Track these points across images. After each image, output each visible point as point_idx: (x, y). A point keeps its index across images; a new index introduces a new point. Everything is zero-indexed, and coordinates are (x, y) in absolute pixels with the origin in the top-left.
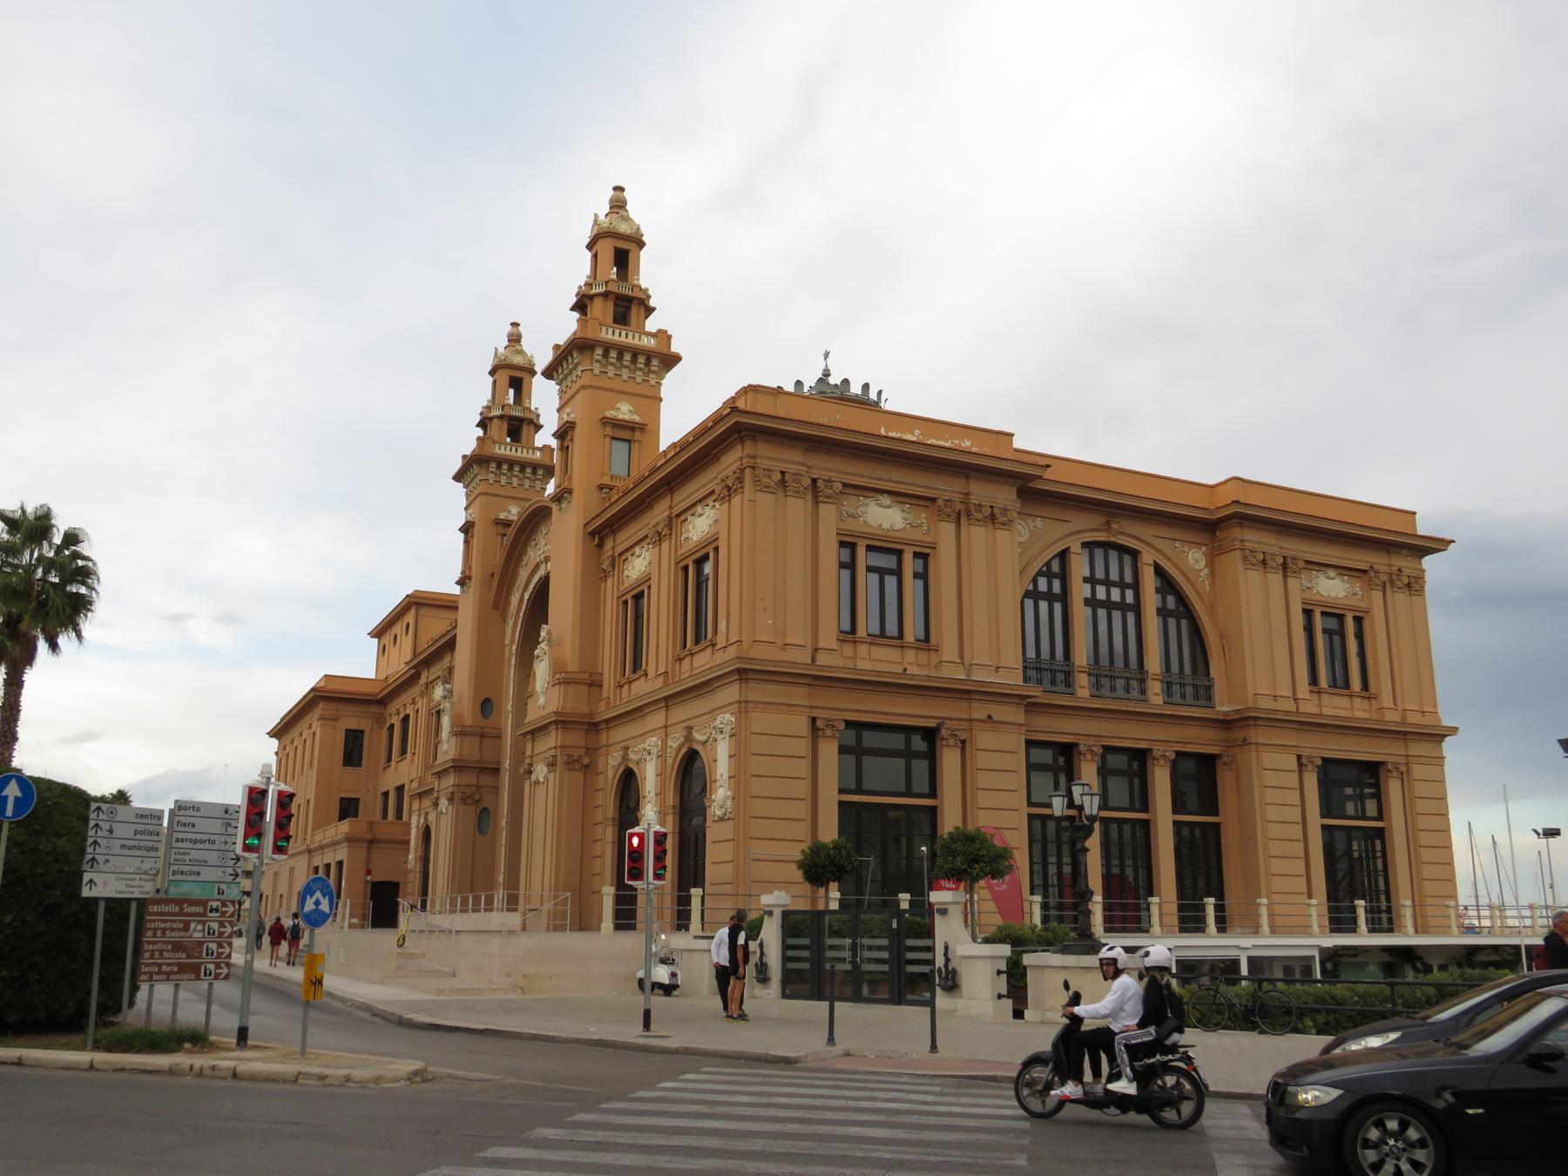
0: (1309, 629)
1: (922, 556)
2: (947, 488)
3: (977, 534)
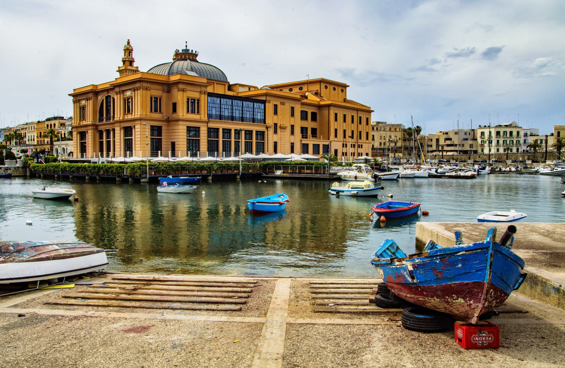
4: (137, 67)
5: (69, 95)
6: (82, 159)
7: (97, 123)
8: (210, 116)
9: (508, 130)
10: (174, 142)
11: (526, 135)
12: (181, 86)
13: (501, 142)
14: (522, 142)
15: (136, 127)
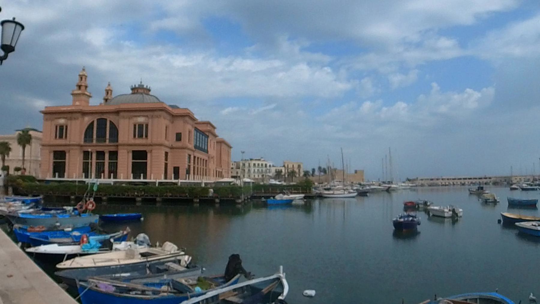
1: (67, 127)
2: (69, 116)
3: (74, 122)
6: (70, 180)
8: (196, 147)
9: (260, 163)
10: (178, 168)
11: (270, 166)
13: (256, 171)
15: (153, 151)
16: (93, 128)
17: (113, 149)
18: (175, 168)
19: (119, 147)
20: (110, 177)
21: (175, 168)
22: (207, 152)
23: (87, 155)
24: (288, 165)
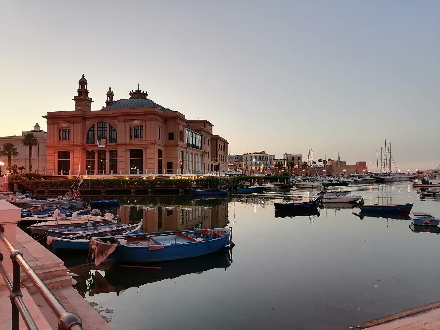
0: (131, 130)
3: (75, 125)
4: (91, 98)
5: (44, 117)
7: (85, 144)
11: (271, 159)
12: (179, 121)
14: (269, 163)
15: (148, 150)
16: (94, 131)
17: (113, 148)
18: (168, 163)
19: (118, 147)
20: (110, 173)
21: (168, 163)
22: (201, 148)
23: (89, 154)
24: (288, 158)
